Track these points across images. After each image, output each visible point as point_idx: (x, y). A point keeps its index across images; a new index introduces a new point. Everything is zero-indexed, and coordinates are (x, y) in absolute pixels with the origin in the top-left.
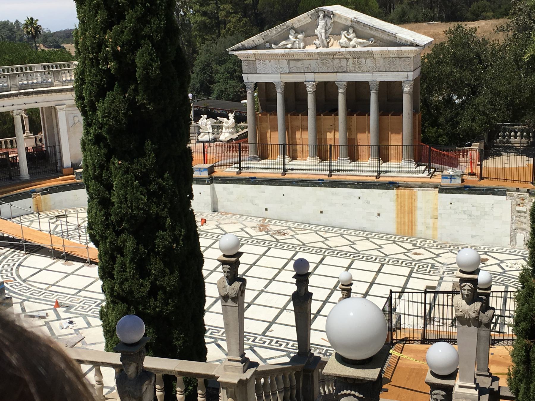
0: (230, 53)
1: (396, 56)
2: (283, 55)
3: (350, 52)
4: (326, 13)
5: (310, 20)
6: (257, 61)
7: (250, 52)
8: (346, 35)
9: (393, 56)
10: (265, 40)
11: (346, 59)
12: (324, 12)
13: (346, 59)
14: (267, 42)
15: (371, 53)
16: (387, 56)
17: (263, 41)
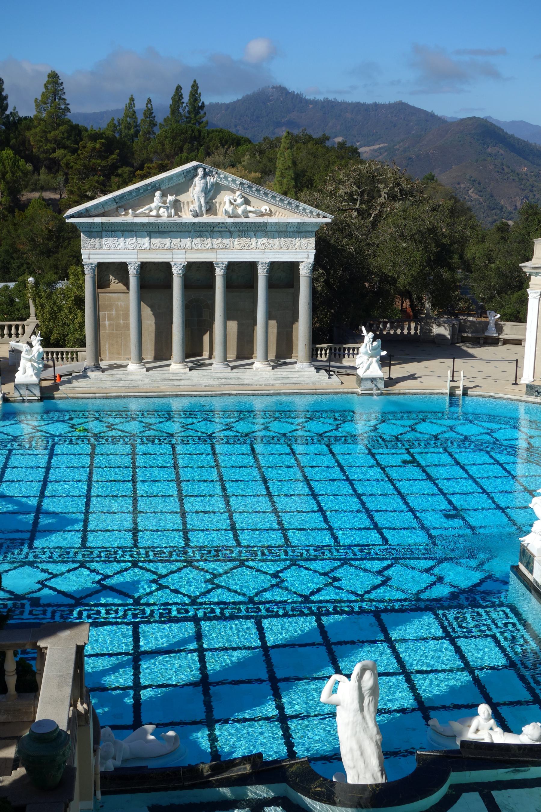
0: (67, 221)
1: (295, 229)
2: (143, 225)
3: (237, 223)
4: (207, 170)
5: (184, 179)
6: (104, 233)
7: (98, 220)
8: (232, 201)
9: (291, 230)
10: (119, 205)
11: (230, 232)
12: (205, 169)
13: (230, 232)
14: (120, 207)
15: (264, 225)
16: (283, 230)
17: (116, 206)
